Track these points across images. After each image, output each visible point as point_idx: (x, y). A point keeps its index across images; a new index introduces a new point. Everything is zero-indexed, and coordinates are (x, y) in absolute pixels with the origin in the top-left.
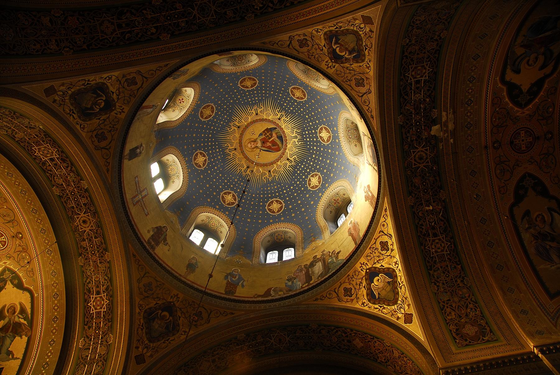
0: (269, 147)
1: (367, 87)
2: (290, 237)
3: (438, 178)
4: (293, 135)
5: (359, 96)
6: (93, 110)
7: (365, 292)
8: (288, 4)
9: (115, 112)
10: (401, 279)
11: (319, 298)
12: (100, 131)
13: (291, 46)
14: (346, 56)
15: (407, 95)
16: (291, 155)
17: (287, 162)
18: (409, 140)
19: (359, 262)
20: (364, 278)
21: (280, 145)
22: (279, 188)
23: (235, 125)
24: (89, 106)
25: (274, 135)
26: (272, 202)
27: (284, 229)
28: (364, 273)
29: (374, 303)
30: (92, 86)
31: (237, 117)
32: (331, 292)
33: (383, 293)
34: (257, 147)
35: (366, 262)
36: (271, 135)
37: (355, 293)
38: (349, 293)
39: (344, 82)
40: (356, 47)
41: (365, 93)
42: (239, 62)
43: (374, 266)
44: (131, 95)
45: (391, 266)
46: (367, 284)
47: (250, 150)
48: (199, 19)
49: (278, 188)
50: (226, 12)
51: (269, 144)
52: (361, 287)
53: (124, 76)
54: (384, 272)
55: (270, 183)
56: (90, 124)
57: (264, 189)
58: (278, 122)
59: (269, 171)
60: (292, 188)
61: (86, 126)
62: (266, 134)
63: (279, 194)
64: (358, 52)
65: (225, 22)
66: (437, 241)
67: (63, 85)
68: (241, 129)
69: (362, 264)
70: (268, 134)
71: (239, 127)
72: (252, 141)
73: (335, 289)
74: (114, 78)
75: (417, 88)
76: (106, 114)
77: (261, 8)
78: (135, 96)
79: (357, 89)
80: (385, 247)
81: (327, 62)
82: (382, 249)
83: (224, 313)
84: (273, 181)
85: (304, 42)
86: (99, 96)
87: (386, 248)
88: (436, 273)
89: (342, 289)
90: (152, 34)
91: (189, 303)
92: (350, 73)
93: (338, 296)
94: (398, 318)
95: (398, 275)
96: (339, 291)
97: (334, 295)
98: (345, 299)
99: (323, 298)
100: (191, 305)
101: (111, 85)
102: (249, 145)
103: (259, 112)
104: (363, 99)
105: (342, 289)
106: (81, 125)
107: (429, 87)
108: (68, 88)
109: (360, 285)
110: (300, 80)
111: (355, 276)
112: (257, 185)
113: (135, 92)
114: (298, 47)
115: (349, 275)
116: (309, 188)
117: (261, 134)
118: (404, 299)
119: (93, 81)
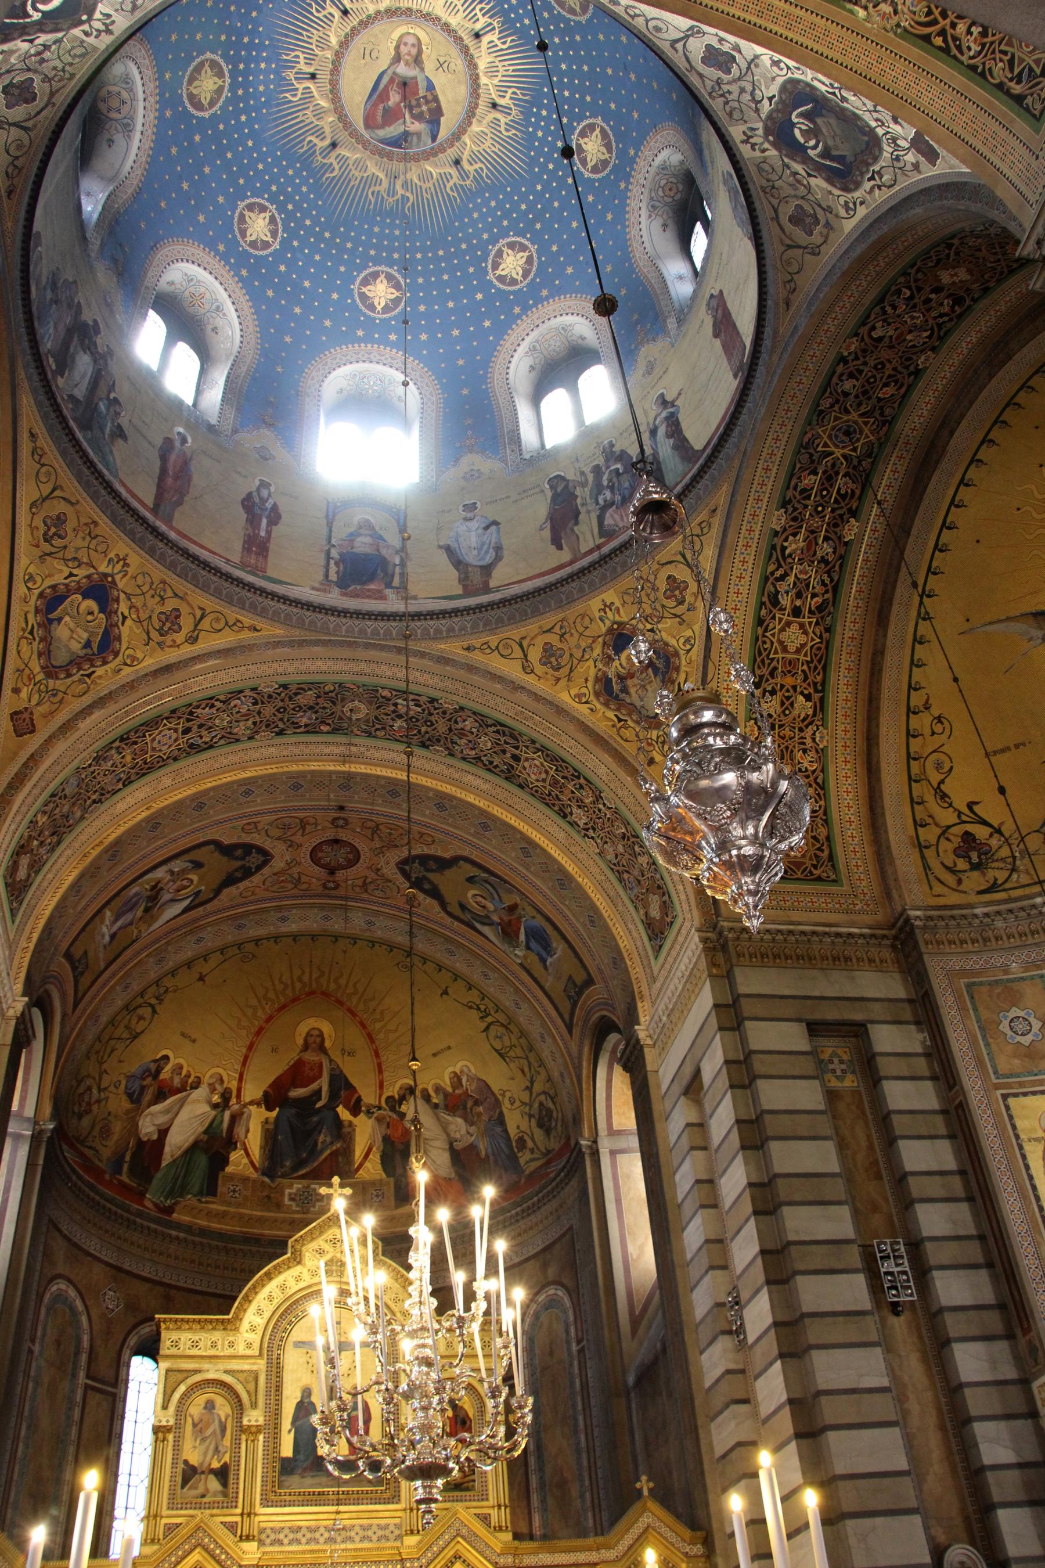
0: (384, 97)
1: (540, 669)
2: (111, 142)
3: (302, 729)
4: (398, 187)
5: (523, 638)
6: (801, 115)
7: (58, 579)
8: (763, 612)
9: (760, 132)
10: (100, 677)
11: (38, 444)
12: (734, 69)
13: (679, 558)
14: (616, 663)
15: (498, 732)
16: (343, 160)
17: (327, 142)
18: (400, 701)
19: (127, 550)
20: (92, 570)
21: (381, 133)
22: (257, 99)
23: (489, 28)
24: (819, 121)
25: (416, 126)
26: (220, 74)
27: (139, 128)
28: (103, 568)
29: (37, 611)
30: (862, 174)
31: (509, 48)
32: (53, 477)
33: (61, 632)
34: (397, 58)
35: (131, 571)
36: (419, 117)
37: (54, 550)
38: (53, 530)
39: (562, 621)
40: (628, 701)
41: (526, 656)
42: (663, 182)
43: (122, 596)
44: (773, 187)
45: (124, 646)
46: (78, 582)
47: (395, 36)
48: (836, 419)
49: (256, 96)
50: (816, 474)
51: (394, 98)
52: (70, 564)
53: (828, 225)
54: (112, 625)
55: (277, 72)
56: (773, 79)
57: (265, 48)
58: (451, 153)
59: (313, 76)
60: (250, 143)
61: (775, 69)
62: (427, 102)
63: (240, 99)
64: (617, 698)
65: (798, 466)
66: (174, 736)
67: (916, 166)
68: (468, 41)
69: (124, 559)
70: (424, 108)
71: (477, 36)
72: (420, 52)
73: (62, 488)
74: (842, 213)
75: (504, 752)
76: (770, 116)
77: (783, 549)
78: (764, 191)
79: (540, 641)
80: (168, 625)
81: (618, 610)
82: (163, 617)
83: (16, 167)
84: (281, 80)
85: (677, 593)
86: (826, 154)
87: (166, 628)
88: (113, 751)
89: (62, 507)
90: (873, 328)
91: (71, 64)
92: (578, 646)
93: (44, 500)
94: (16, 691)
95: (107, 667)
96: (55, 502)
97: (46, 489)
98: (38, 522)
99: (37, 457)
100: (63, 70)
101: (830, 193)
102: (411, 40)
103: (499, 116)
104: (517, 648)
105: (62, 507)
106: (788, 68)
107: (496, 767)
108: (898, 159)
109: (75, 559)
110: (547, 298)
111: (94, 542)
112: (282, 27)
113: (775, 202)
114: (670, 570)
115: (95, 523)
116: (241, 205)
117: (430, 87)
118: (60, 695)
119: (872, 189)
